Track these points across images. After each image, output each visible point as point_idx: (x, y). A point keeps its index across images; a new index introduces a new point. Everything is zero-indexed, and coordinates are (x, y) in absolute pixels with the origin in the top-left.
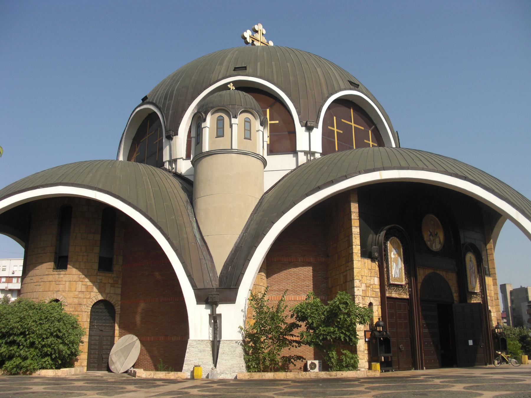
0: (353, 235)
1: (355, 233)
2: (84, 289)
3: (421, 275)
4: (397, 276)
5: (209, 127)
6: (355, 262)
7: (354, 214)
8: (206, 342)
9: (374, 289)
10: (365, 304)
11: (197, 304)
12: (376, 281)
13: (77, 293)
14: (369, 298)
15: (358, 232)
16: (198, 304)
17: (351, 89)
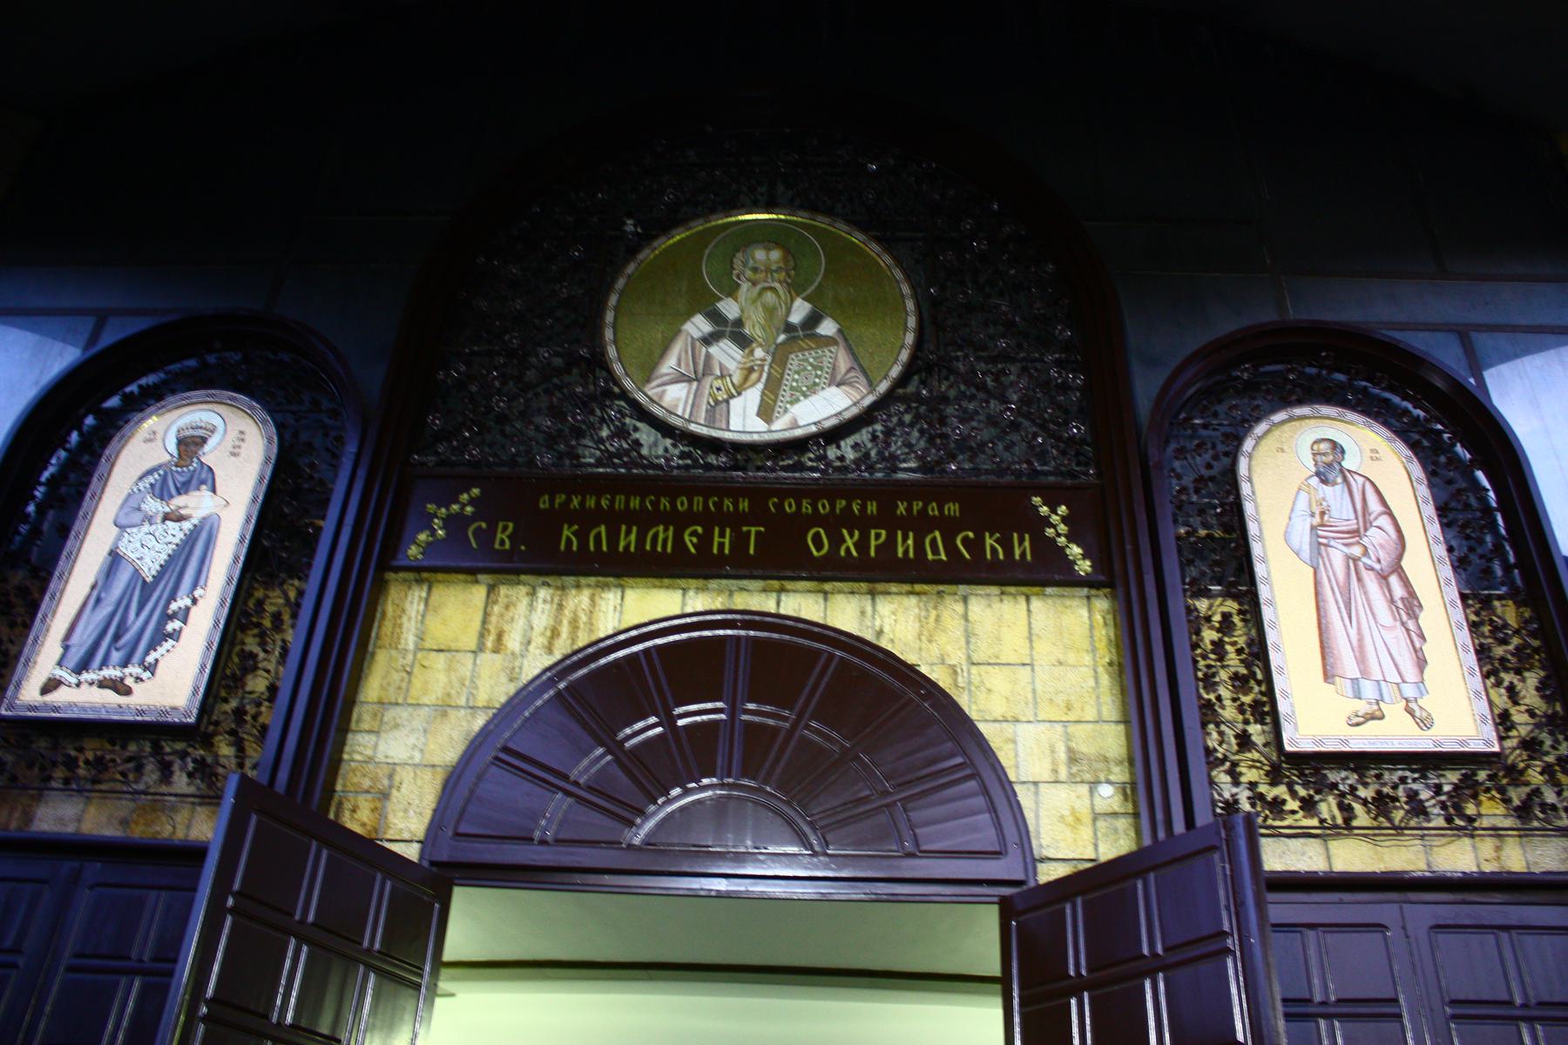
3: (513, 642)
4: (116, 656)
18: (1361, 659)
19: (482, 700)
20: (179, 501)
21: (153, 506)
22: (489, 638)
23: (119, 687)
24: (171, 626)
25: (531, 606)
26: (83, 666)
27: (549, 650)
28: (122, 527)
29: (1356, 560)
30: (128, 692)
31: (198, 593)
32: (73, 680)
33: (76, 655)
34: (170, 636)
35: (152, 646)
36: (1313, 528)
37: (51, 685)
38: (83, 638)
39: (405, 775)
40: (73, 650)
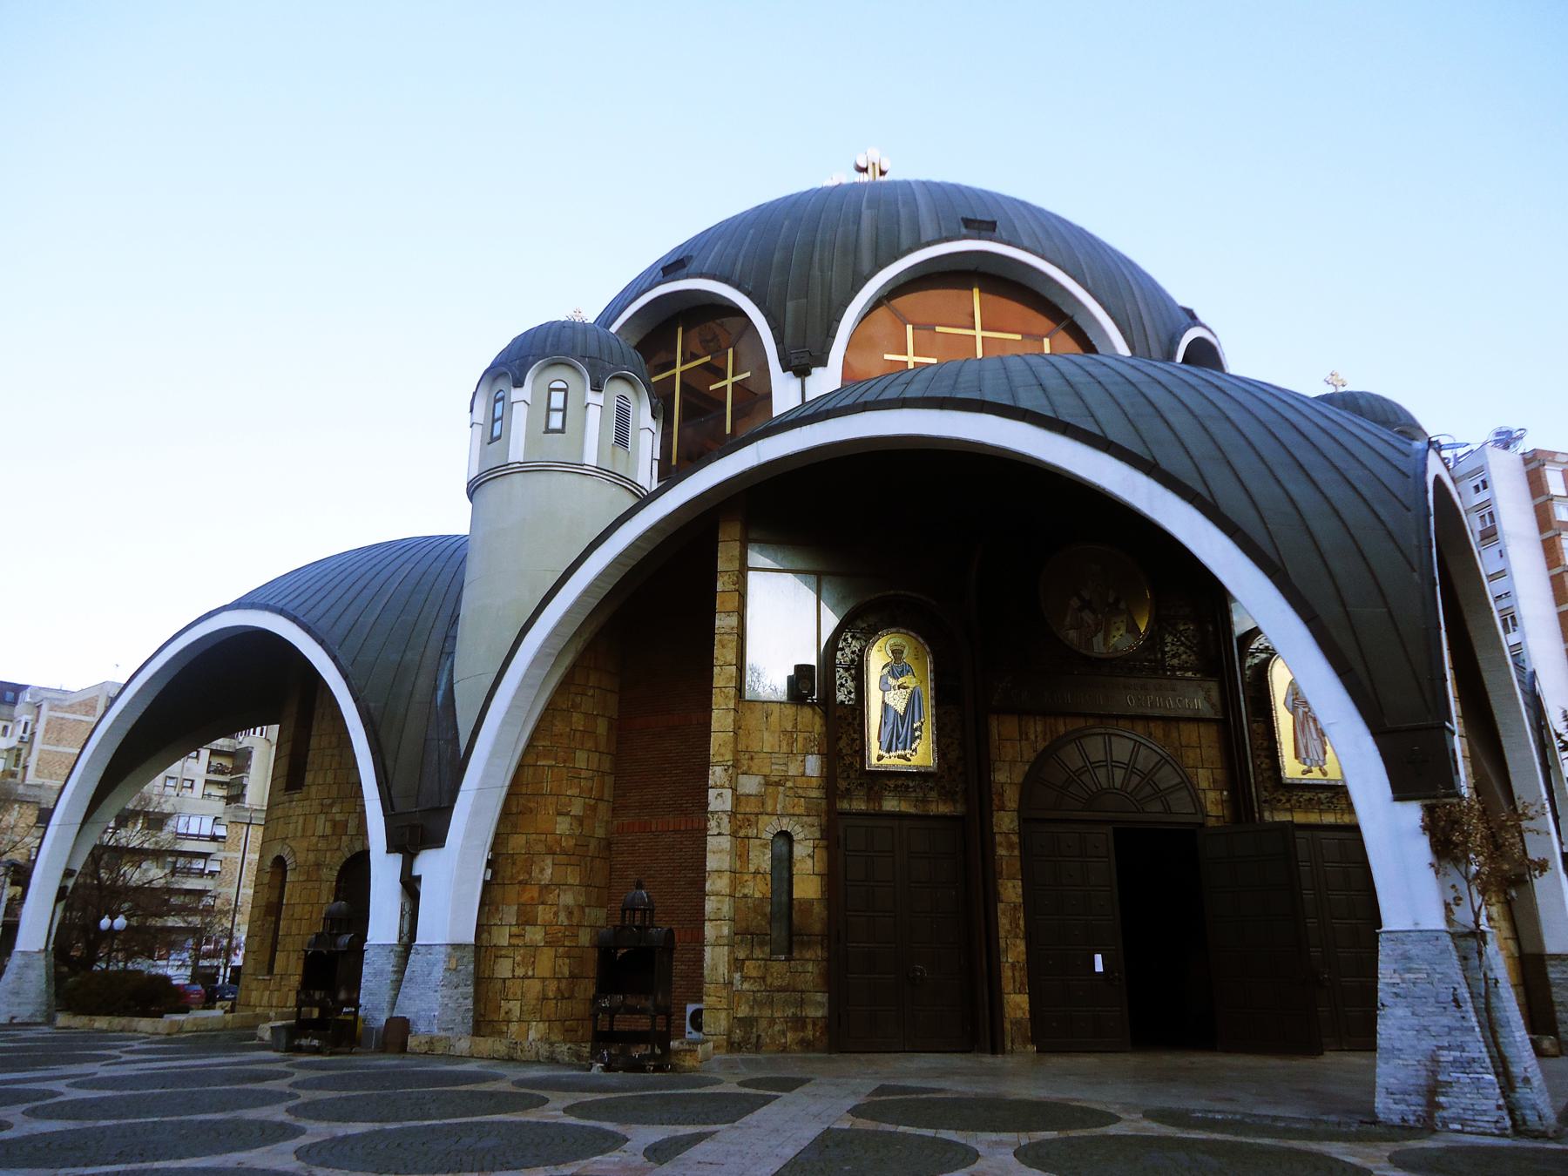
0: (717, 638)
1: (723, 631)
2: (328, 831)
3: (1033, 737)
4: (900, 746)
5: (482, 422)
6: (715, 714)
7: (726, 578)
8: (390, 948)
9: (800, 791)
10: (757, 838)
11: (388, 852)
12: (813, 765)
13: (314, 840)
14: (775, 817)
15: (732, 628)
16: (391, 852)
17: (965, 237)
18: (1307, 752)
19: (1026, 758)
20: (901, 680)
21: (891, 681)
22: (1024, 735)
23: (904, 757)
24: (917, 734)
25: (1035, 724)
26: (889, 750)
27: (1045, 740)
28: (884, 691)
29: (1306, 713)
30: (910, 760)
31: (922, 720)
32: (887, 755)
33: (885, 746)
34: (918, 737)
35: (912, 743)
36: (1293, 700)
37: (880, 758)
38: (885, 738)
39: (1007, 787)
40: (883, 744)
